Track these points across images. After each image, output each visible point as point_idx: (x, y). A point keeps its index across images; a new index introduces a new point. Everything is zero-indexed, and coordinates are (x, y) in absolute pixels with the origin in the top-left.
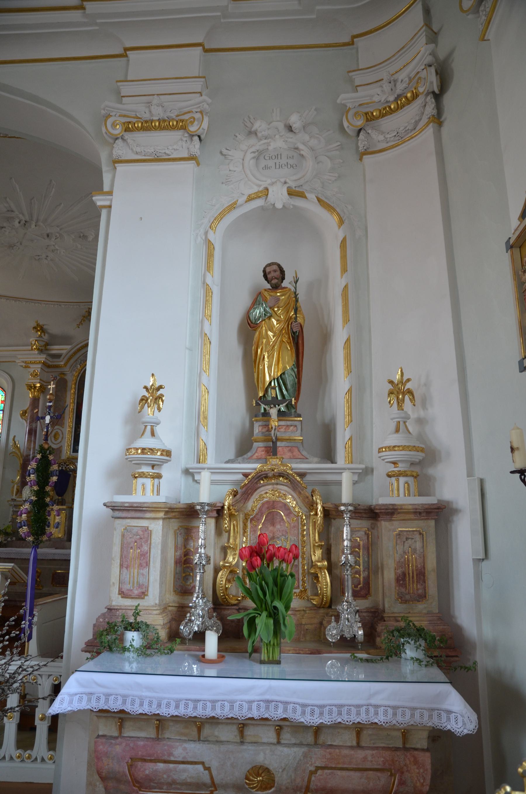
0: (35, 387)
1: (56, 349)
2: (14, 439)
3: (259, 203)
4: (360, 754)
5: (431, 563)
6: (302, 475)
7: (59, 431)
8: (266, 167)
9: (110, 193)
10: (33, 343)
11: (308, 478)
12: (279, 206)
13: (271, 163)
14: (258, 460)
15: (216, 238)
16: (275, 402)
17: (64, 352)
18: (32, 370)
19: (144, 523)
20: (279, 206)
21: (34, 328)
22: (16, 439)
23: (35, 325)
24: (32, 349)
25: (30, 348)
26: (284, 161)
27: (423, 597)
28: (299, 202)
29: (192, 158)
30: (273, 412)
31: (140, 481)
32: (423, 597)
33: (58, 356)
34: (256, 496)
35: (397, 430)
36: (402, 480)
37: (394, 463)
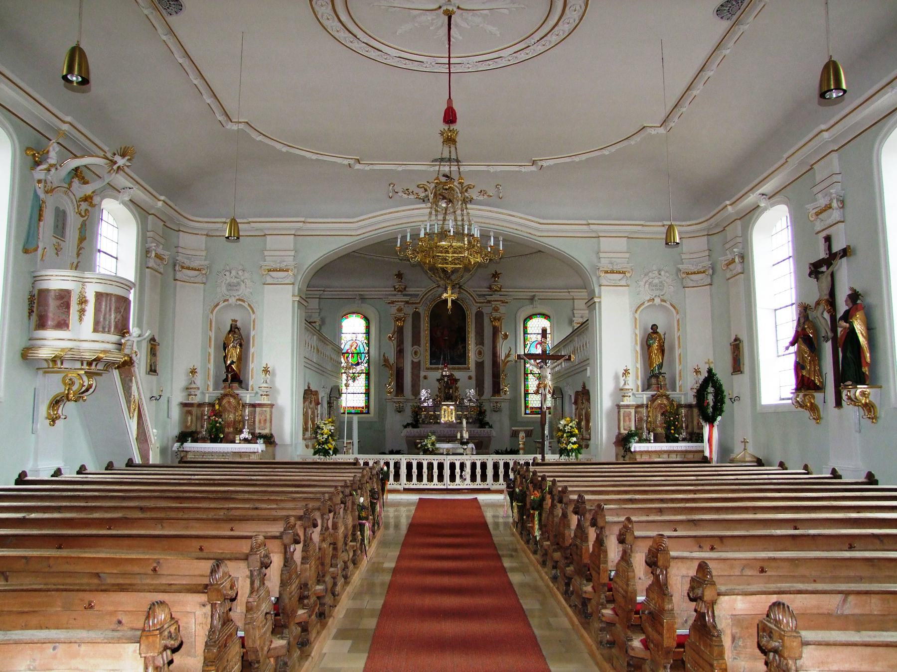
1: (411, 290)
2: (384, 355)
8: (652, 290)
9: (600, 297)
10: (397, 287)
12: (657, 304)
13: (654, 288)
14: (654, 391)
15: (637, 316)
18: (398, 306)
19: (629, 410)
20: (657, 304)
21: (396, 275)
22: (386, 356)
23: (397, 273)
25: (393, 289)
28: (664, 303)
29: (628, 286)
31: (626, 398)
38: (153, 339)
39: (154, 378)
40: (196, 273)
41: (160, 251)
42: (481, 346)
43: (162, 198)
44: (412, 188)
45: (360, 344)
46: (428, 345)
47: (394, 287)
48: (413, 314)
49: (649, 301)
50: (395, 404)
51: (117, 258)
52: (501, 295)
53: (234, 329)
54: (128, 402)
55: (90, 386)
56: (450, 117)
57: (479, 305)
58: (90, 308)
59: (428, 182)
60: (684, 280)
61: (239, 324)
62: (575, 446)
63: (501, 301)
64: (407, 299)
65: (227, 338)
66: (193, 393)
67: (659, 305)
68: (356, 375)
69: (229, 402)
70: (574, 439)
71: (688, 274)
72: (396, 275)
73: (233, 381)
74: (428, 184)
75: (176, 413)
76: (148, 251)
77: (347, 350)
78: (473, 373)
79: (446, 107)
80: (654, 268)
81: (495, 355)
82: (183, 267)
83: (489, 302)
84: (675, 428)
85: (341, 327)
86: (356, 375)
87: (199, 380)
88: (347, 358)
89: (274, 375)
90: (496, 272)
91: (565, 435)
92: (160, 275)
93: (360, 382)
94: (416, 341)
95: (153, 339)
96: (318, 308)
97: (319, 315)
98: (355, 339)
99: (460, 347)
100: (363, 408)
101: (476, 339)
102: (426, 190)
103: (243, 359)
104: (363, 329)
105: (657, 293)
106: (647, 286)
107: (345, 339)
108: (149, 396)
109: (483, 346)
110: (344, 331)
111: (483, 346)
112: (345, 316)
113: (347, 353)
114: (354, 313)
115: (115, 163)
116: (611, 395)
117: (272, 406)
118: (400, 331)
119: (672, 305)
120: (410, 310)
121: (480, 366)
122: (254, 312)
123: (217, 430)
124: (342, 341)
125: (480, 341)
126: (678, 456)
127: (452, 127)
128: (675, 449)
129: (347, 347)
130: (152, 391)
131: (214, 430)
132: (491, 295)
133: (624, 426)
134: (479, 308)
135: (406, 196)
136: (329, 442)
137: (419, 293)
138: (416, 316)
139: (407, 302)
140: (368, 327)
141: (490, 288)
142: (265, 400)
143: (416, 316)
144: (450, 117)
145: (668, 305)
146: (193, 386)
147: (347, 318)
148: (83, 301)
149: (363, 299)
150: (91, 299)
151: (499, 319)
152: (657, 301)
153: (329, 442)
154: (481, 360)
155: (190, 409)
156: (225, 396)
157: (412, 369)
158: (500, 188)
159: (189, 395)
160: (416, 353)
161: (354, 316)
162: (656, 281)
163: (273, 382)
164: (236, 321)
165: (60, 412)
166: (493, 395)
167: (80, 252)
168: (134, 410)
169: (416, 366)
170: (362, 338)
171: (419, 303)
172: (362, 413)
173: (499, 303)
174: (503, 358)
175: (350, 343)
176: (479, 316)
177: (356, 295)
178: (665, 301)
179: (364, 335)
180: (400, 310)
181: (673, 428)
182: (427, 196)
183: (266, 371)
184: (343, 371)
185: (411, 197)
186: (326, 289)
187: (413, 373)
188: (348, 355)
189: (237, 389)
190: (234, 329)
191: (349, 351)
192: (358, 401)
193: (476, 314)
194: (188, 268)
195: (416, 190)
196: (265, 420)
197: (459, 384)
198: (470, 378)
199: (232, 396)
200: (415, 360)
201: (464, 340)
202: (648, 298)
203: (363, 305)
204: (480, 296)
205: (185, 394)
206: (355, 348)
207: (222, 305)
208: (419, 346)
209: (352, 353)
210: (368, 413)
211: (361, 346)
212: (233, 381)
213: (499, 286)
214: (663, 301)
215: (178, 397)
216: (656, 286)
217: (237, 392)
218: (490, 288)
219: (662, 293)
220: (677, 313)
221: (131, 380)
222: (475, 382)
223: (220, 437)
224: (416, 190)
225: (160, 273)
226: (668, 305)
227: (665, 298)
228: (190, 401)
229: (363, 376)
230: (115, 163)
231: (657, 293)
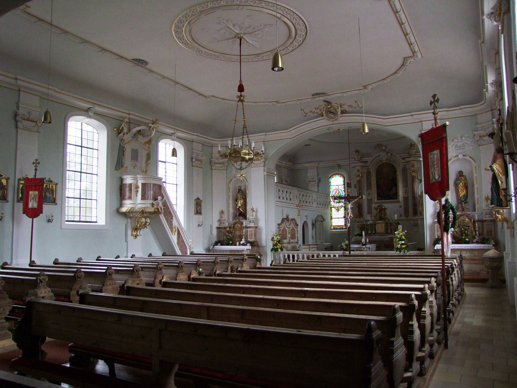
0: (359, 176)
1: (365, 159)
3: (457, 158)
4: (479, 255)
5: (493, 229)
6: (469, 215)
7: (370, 192)
11: (470, 215)
12: (461, 159)
14: (460, 212)
16: (463, 201)
17: (369, 160)
18: (357, 169)
20: (461, 159)
21: (355, 151)
24: (355, 160)
26: (461, 148)
27: (491, 235)
30: (463, 203)
32: (491, 235)
33: (366, 162)
34: (460, 219)
35: (487, 206)
36: (488, 215)
37: (486, 212)
38: (198, 199)
39: (198, 216)
40: (221, 165)
41: (200, 158)
42: (407, 188)
43: (195, 134)
44: (314, 110)
45: (340, 191)
46: (376, 189)
47: (355, 158)
48: (367, 172)
49: (454, 157)
50: (357, 224)
51: (177, 164)
52: (415, 157)
53: (240, 190)
54: (171, 227)
55: (146, 222)
56: (241, 88)
57: (403, 164)
58: (140, 190)
59: (319, 106)
60: (479, 141)
61: (242, 188)
62: (403, 246)
63: (415, 160)
64: (361, 164)
65: (237, 195)
66: (222, 222)
67: (462, 158)
68: (339, 208)
69: (238, 226)
70: (403, 242)
71: (480, 137)
72: (355, 151)
73: (239, 216)
74: (319, 107)
75: (215, 232)
76: (192, 159)
78: (402, 204)
79: (239, 84)
80: (459, 136)
81: (413, 192)
82: (215, 163)
83: (408, 162)
84: (465, 235)
85: (330, 183)
86: (339, 208)
87: (225, 217)
89: (257, 211)
90: (411, 144)
91: (397, 240)
92: (201, 169)
93: (341, 212)
94: (369, 187)
95: (198, 199)
97: (317, 177)
99: (394, 189)
100: (343, 226)
101: (403, 184)
102: (321, 110)
103: (245, 204)
104: (342, 183)
105: (461, 151)
106: (454, 148)
107: (332, 189)
108: (197, 225)
109: (408, 188)
110: (332, 184)
111: (408, 188)
112: (332, 176)
115: (151, 127)
116: (432, 216)
117: (256, 227)
118: (359, 182)
119: (470, 157)
120: (365, 171)
121: (406, 199)
122: (247, 182)
123: (228, 240)
124: (331, 190)
125: (406, 186)
126: (468, 252)
127: (243, 93)
128: (463, 248)
130: (199, 222)
131: (227, 239)
132: (410, 158)
133: (437, 234)
134: (404, 166)
135: (312, 114)
136: (277, 245)
137: (368, 160)
138: (369, 173)
139: (362, 166)
140: (344, 181)
141: (409, 153)
142: (252, 225)
143: (369, 173)
144: (241, 88)
145: (468, 158)
146: (222, 219)
147: (333, 177)
148: (137, 187)
149: (339, 166)
150: (140, 185)
151: (414, 171)
152: (461, 156)
153: (277, 245)
154: (406, 196)
155: (220, 230)
156: (236, 223)
157: (368, 203)
158: (358, 103)
159: (221, 223)
160: (369, 194)
161: (337, 176)
162: (460, 144)
163: (256, 215)
164: (241, 187)
165: (138, 233)
166: (413, 217)
167: (148, 165)
168: (175, 231)
169: (370, 202)
170: (342, 188)
171: (369, 166)
172: (342, 229)
173: (415, 162)
174: (420, 194)
175: (335, 191)
176: (405, 170)
178: (465, 156)
179: (343, 186)
180: (358, 171)
181: (464, 235)
182: (322, 113)
183: (253, 210)
184: (332, 206)
185: (315, 114)
187: (368, 206)
189: (242, 220)
190: (240, 190)
192: (340, 222)
193: (403, 169)
194: (218, 163)
195: (316, 111)
196: (252, 234)
197: (387, 211)
198: (400, 207)
199: (239, 223)
200: (369, 198)
201: (396, 185)
202: (455, 155)
203: (340, 170)
204: (403, 159)
205: (219, 223)
206: (338, 194)
207: (234, 180)
208: (371, 189)
210: (346, 229)
211: (341, 192)
212: (239, 216)
213: (414, 152)
214: (464, 156)
215: (216, 224)
216: (460, 147)
217: (242, 221)
218: (409, 153)
219: (464, 151)
220: (475, 162)
221: (172, 218)
222: (403, 209)
223: (230, 243)
224: (316, 111)
225: (202, 168)
226: (468, 158)
227: (466, 153)
228: (221, 226)
229: (343, 208)
230: (151, 127)
231: (461, 151)
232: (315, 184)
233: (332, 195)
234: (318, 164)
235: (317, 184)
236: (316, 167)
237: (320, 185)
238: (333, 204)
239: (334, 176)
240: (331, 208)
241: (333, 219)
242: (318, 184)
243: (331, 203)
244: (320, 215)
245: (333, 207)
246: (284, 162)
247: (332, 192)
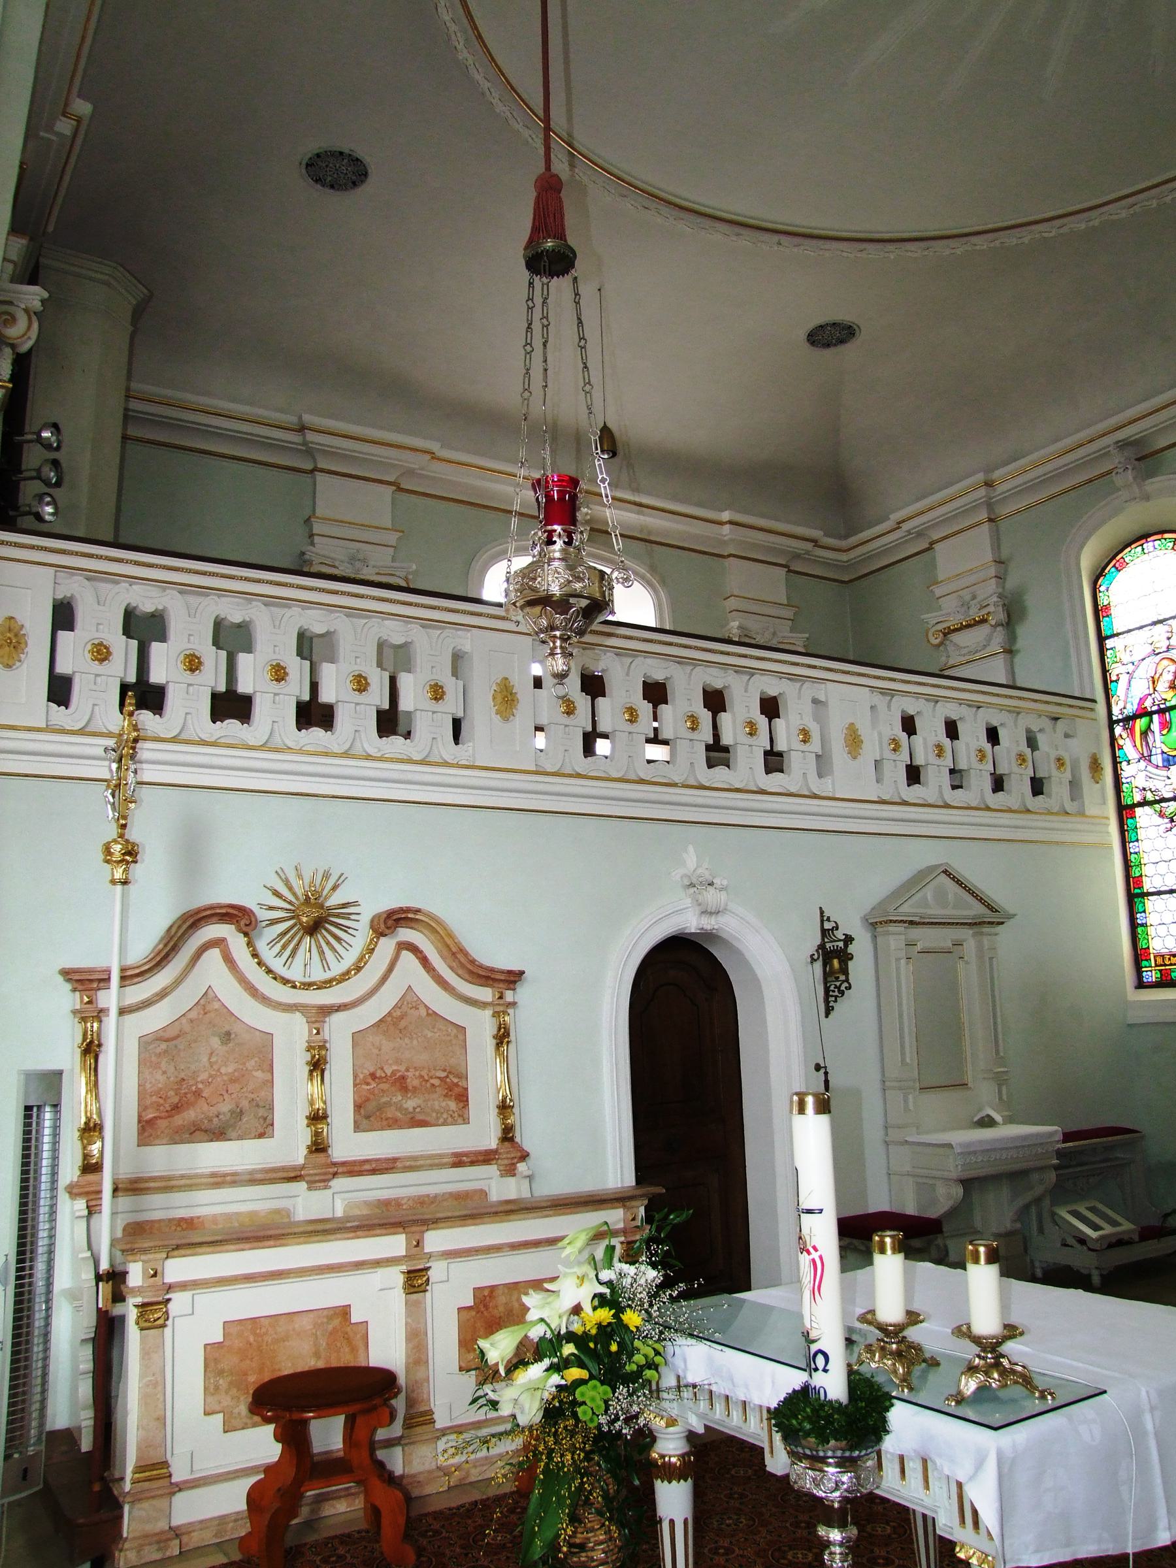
77: (1142, 700)
88: (1145, 734)
96: (989, 556)
98: (1163, 645)
107: (1126, 658)
113: (1142, 713)
114: (1144, 537)
129: (1140, 688)
161: (1148, 546)
175: (1146, 670)
177: (1104, 455)
184: (1138, 798)
186: (996, 474)
188: (1145, 720)
191: (1148, 704)
203: (1154, 484)
209: (1161, 712)
232: (989, 639)
233: (1131, 709)
234: (989, 484)
235: (999, 637)
236: (983, 515)
237: (1020, 644)
238: (1140, 782)
239: (1127, 555)
240: (1125, 811)
241: (1151, 904)
242: (1012, 637)
243: (1127, 771)
244: (930, 869)
245: (1144, 803)
246: (726, 516)
247: (1124, 679)
